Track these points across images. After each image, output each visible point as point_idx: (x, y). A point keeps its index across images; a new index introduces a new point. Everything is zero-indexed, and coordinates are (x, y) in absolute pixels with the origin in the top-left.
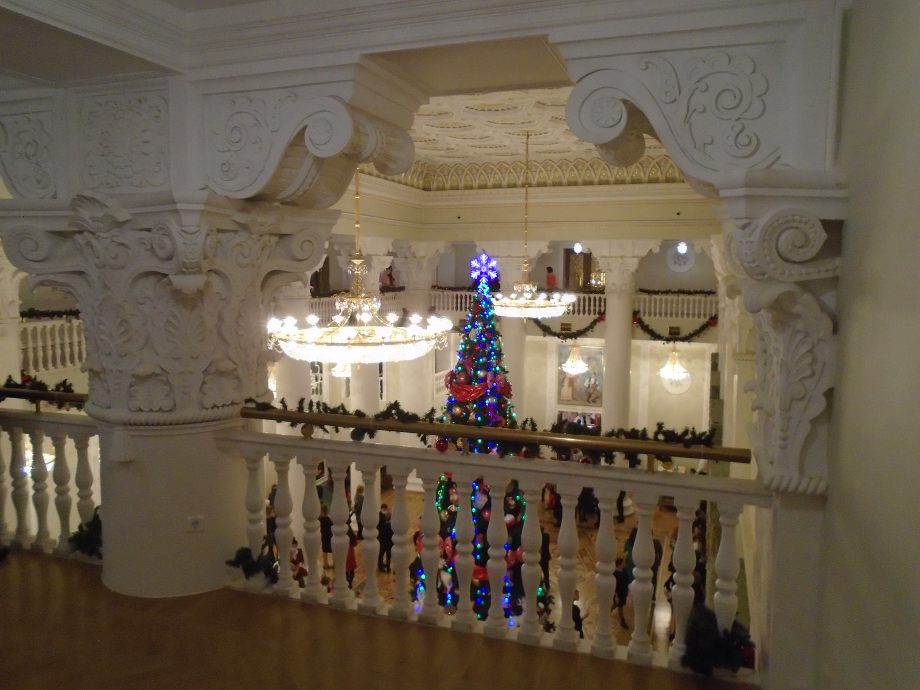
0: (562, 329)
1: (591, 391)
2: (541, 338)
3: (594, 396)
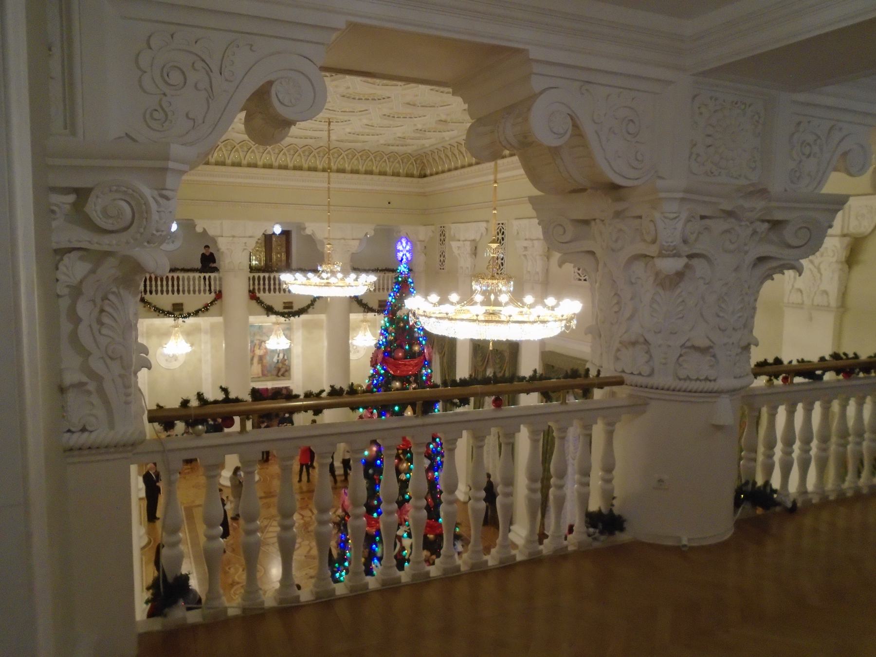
0: (285, 308)
1: (280, 365)
2: (264, 318)
3: (283, 370)
